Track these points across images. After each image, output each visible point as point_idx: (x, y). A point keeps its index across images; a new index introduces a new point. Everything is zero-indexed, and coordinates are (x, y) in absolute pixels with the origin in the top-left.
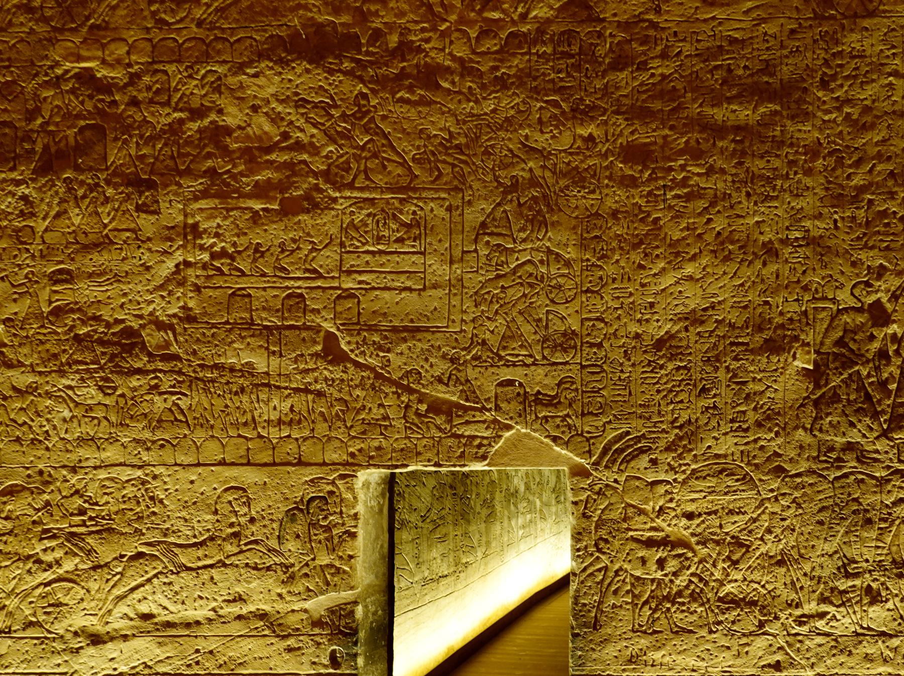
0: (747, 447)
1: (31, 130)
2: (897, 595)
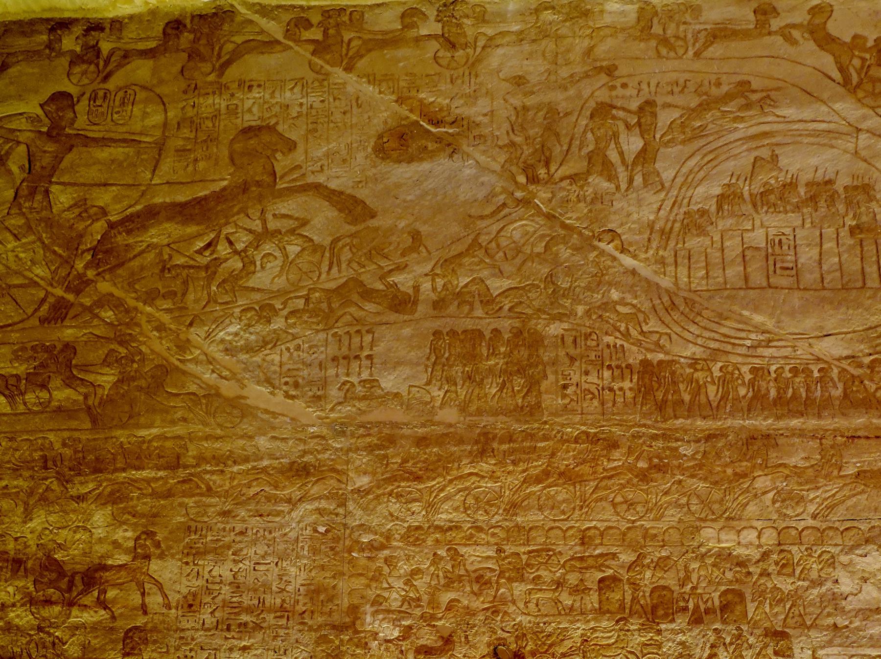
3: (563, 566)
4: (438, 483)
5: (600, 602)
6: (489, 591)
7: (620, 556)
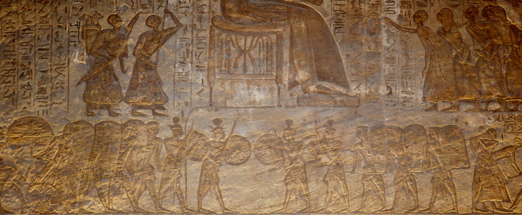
0: (47, 108)
2: (129, 190)
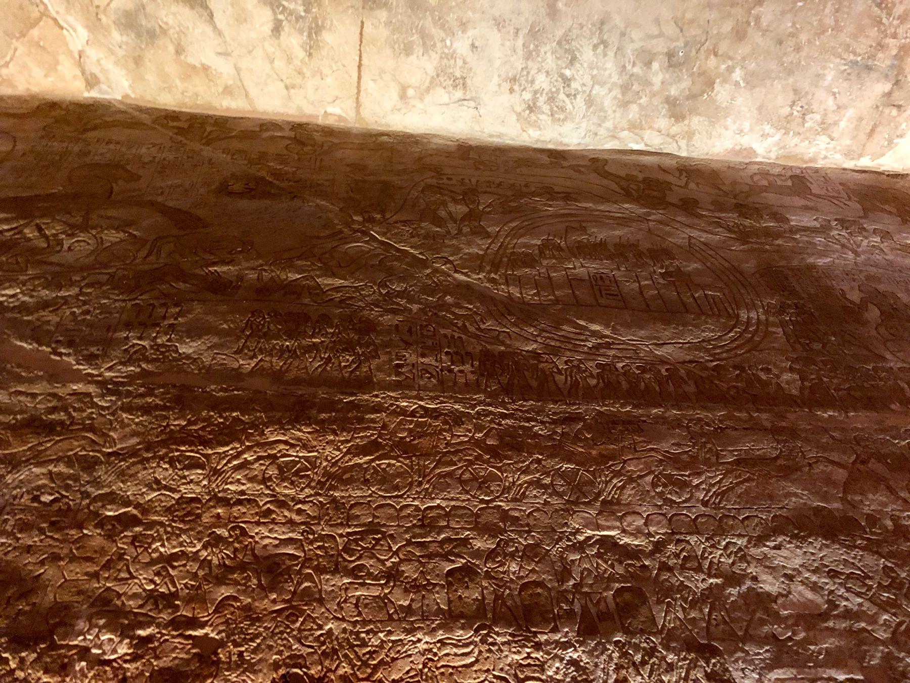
1: (566, 591)
3: (396, 553)
4: (232, 449)
5: (450, 602)
6: (286, 586)
7: (474, 542)
